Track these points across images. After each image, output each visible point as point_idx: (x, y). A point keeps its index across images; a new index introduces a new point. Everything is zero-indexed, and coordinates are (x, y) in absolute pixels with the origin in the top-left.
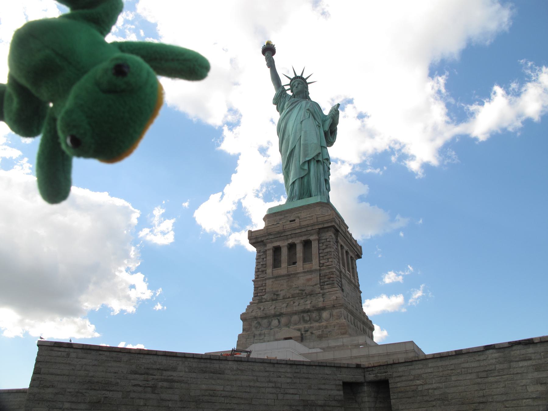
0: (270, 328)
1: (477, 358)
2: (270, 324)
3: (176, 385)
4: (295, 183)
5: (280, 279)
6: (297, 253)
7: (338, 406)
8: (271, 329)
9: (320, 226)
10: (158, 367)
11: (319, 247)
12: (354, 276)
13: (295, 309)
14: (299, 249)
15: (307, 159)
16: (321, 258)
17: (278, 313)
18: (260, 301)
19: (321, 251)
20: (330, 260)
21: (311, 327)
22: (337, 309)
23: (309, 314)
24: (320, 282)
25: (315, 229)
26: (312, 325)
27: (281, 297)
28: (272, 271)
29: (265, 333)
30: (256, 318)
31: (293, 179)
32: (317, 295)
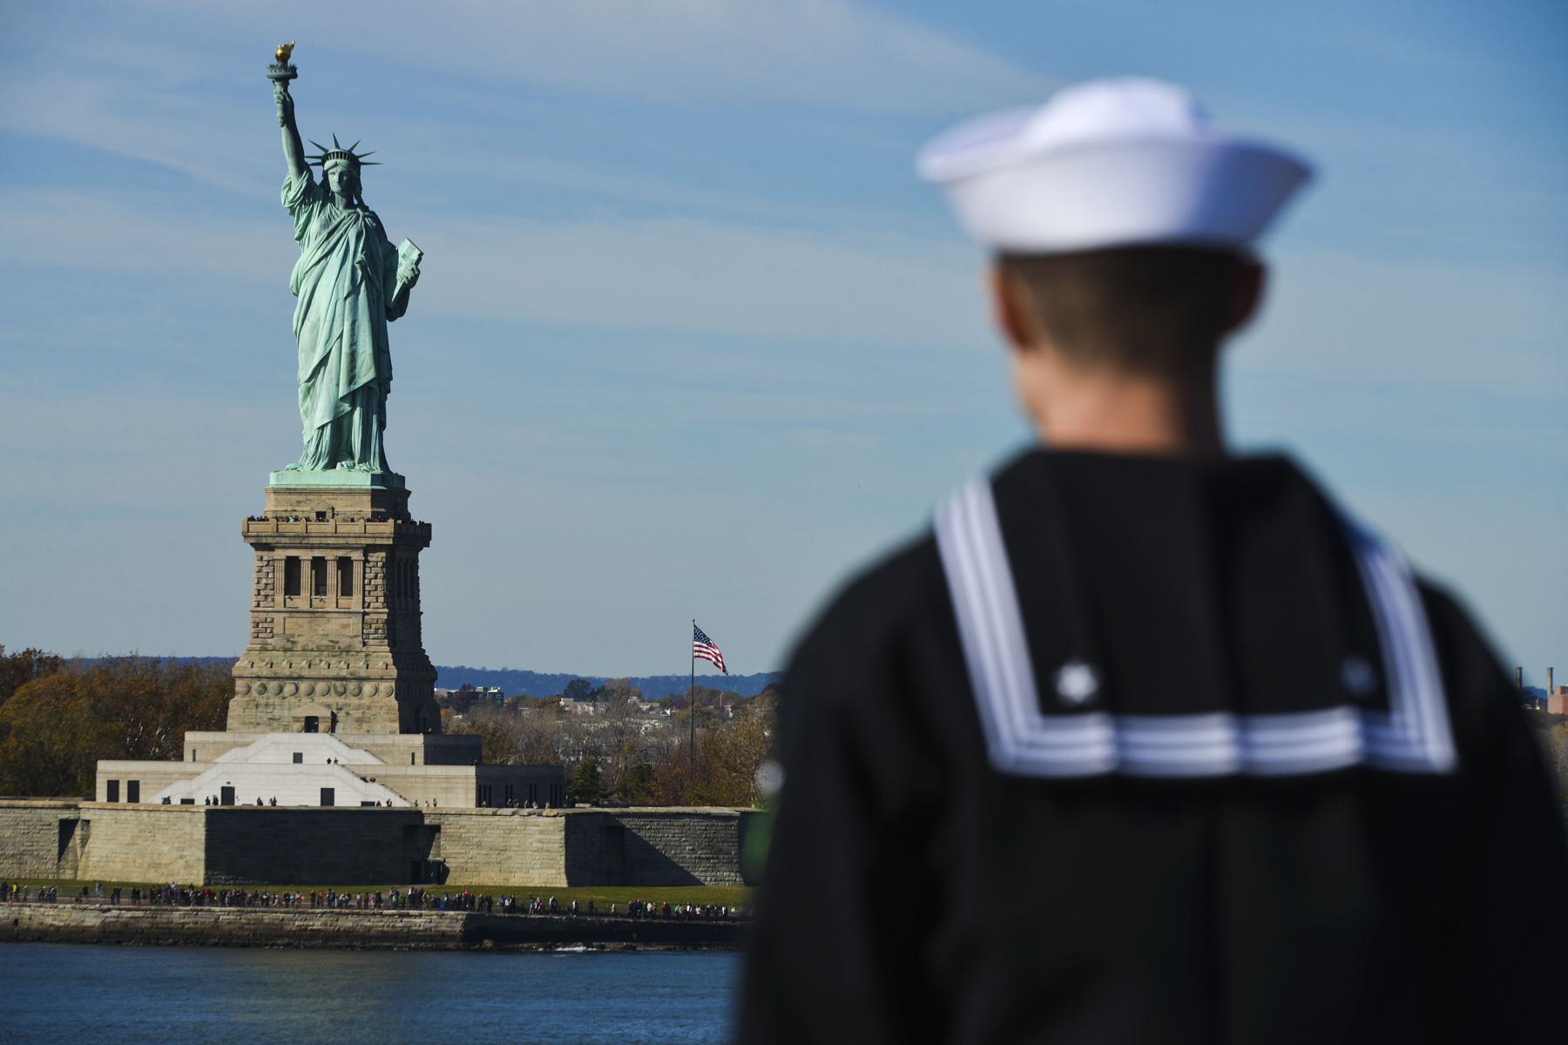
1: (507, 818)
2: (281, 690)
5: (298, 615)
8: (284, 698)
9: (370, 541)
11: (364, 573)
12: (412, 597)
18: (264, 649)
19: (366, 581)
21: (346, 705)
23: (344, 683)
24: (363, 633)
26: (348, 701)
27: (299, 647)
28: (285, 599)
30: (259, 678)
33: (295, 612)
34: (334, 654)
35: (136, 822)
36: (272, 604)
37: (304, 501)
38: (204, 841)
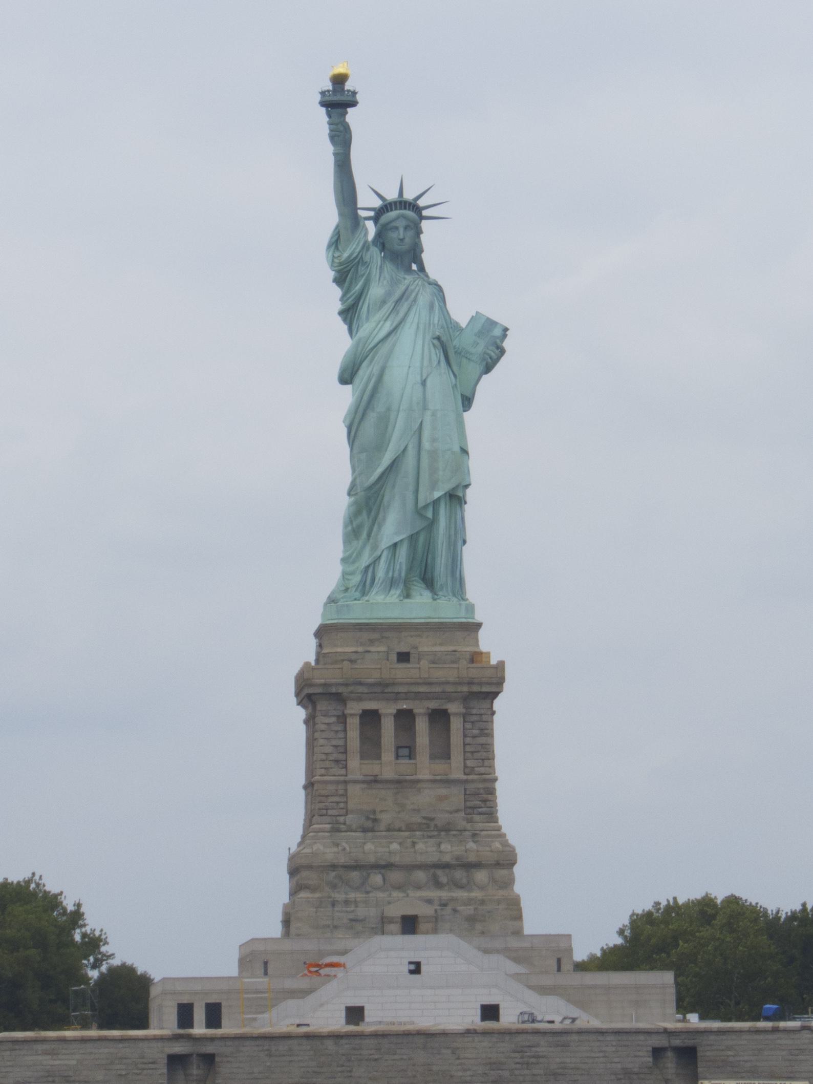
3: (541, 1060)
5: (380, 786)
7: (648, 1074)
8: (367, 893)
10: (528, 1044)
13: (420, 859)
14: (422, 726)
15: (437, 494)
16: (469, 755)
17: (383, 863)
18: (335, 830)
19: (468, 740)
20: (486, 763)
21: (453, 899)
22: (503, 869)
23: (447, 871)
24: (466, 807)
25: (461, 692)
27: (382, 826)
28: (361, 764)
29: (358, 899)
30: (334, 867)
32: (461, 835)
33: (374, 781)
34: (429, 834)
35: (312, 1053)
36: (343, 772)
37: (380, 639)
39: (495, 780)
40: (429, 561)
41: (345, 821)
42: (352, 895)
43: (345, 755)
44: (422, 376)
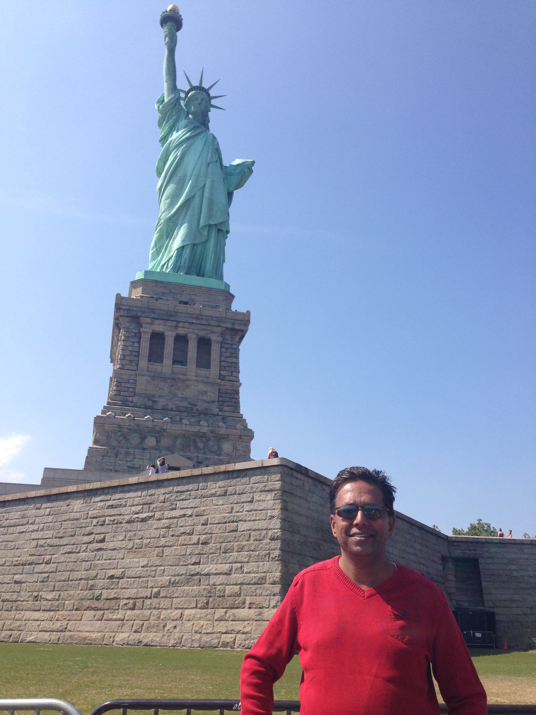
0: (142, 447)
4: (186, 247)
6: (189, 350)
8: (144, 449)
11: (221, 352)
15: (212, 223)
16: (222, 368)
19: (223, 358)
20: (234, 374)
21: (207, 459)
23: (204, 439)
24: (218, 401)
27: (159, 406)
28: (148, 364)
29: (135, 453)
31: (183, 241)
32: (215, 417)
34: (193, 414)
35: (50, 519)
37: (168, 293)
38: (278, 533)
39: (241, 384)
40: (203, 264)
41: (133, 400)
42: (132, 451)
43: (138, 358)
44: (206, 161)
